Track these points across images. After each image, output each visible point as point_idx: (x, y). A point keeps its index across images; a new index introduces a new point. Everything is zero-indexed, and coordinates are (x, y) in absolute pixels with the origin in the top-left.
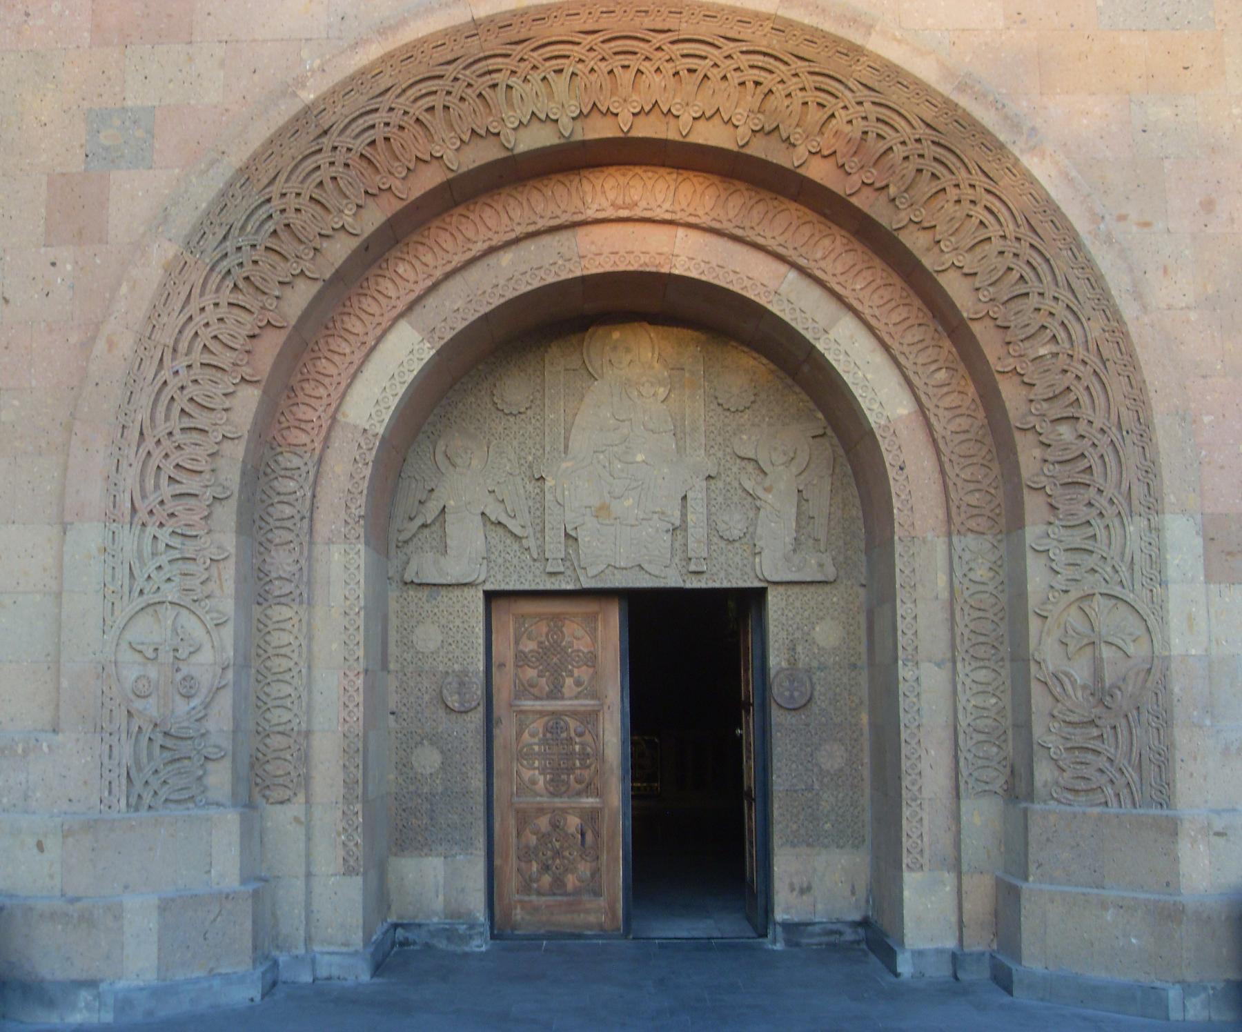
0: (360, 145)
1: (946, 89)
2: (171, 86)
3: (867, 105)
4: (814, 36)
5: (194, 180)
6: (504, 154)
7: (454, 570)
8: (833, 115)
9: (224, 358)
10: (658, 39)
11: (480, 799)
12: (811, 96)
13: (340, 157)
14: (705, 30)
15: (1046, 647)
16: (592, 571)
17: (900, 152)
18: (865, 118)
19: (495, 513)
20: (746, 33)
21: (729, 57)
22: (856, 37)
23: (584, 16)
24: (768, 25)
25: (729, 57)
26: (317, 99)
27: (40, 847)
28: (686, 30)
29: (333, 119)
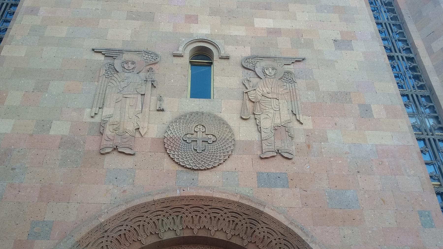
0: (116, 236)
1: (286, 223)
2: (60, 215)
3: (264, 228)
4: (249, 208)
5: (62, 244)
6: (160, 240)
8: (255, 231)
10: (206, 208)
12: (248, 225)
13: (109, 239)
14: (219, 205)
18: (264, 232)
20: (230, 207)
21: (226, 213)
22: (261, 209)
23: (185, 200)
24: (236, 205)
25: (226, 213)
26: (104, 221)
28: (214, 205)
29: (109, 227)
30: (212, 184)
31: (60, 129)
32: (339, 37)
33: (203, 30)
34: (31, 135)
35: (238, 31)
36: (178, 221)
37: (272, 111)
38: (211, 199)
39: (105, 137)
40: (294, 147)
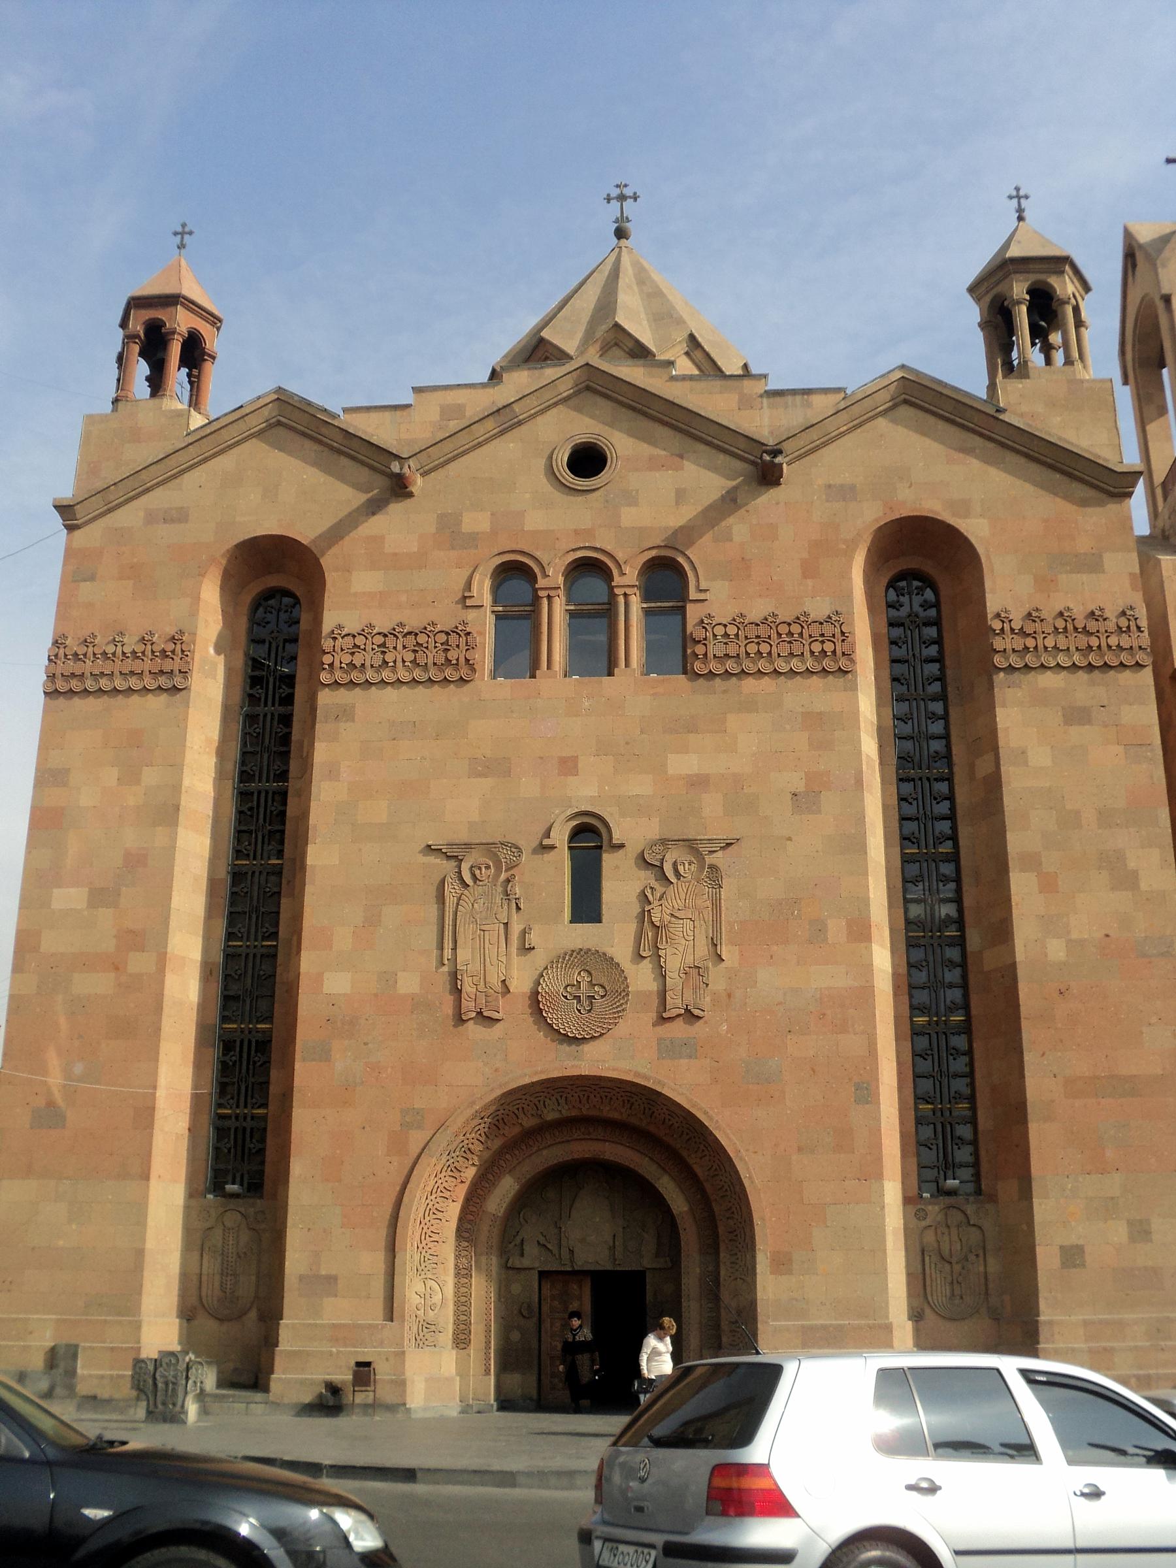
7: (526, 1262)
9: (447, 1194)
11: (536, 1352)
14: (609, 1084)
15: (725, 1295)
16: (580, 1263)
17: (676, 1125)
19: (542, 1240)
27: (387, 1359)
28: (603, 1084)
30: (599, 1060)
31: (408, 984)
32: (800, 786)
33: (585, 792)
34: (376, 995)
35: (640, 786)
36: (562, 1101)
37: (683, 942)
38: (600, 1078)
39: (464, 995)
40: (708, 999)
